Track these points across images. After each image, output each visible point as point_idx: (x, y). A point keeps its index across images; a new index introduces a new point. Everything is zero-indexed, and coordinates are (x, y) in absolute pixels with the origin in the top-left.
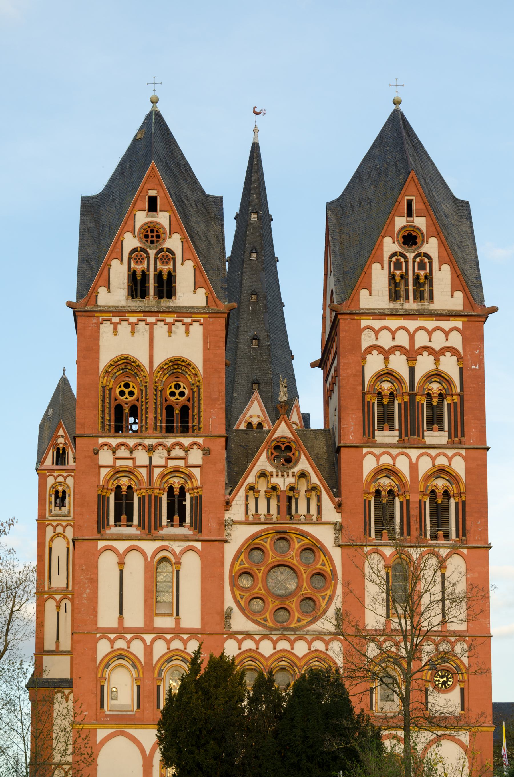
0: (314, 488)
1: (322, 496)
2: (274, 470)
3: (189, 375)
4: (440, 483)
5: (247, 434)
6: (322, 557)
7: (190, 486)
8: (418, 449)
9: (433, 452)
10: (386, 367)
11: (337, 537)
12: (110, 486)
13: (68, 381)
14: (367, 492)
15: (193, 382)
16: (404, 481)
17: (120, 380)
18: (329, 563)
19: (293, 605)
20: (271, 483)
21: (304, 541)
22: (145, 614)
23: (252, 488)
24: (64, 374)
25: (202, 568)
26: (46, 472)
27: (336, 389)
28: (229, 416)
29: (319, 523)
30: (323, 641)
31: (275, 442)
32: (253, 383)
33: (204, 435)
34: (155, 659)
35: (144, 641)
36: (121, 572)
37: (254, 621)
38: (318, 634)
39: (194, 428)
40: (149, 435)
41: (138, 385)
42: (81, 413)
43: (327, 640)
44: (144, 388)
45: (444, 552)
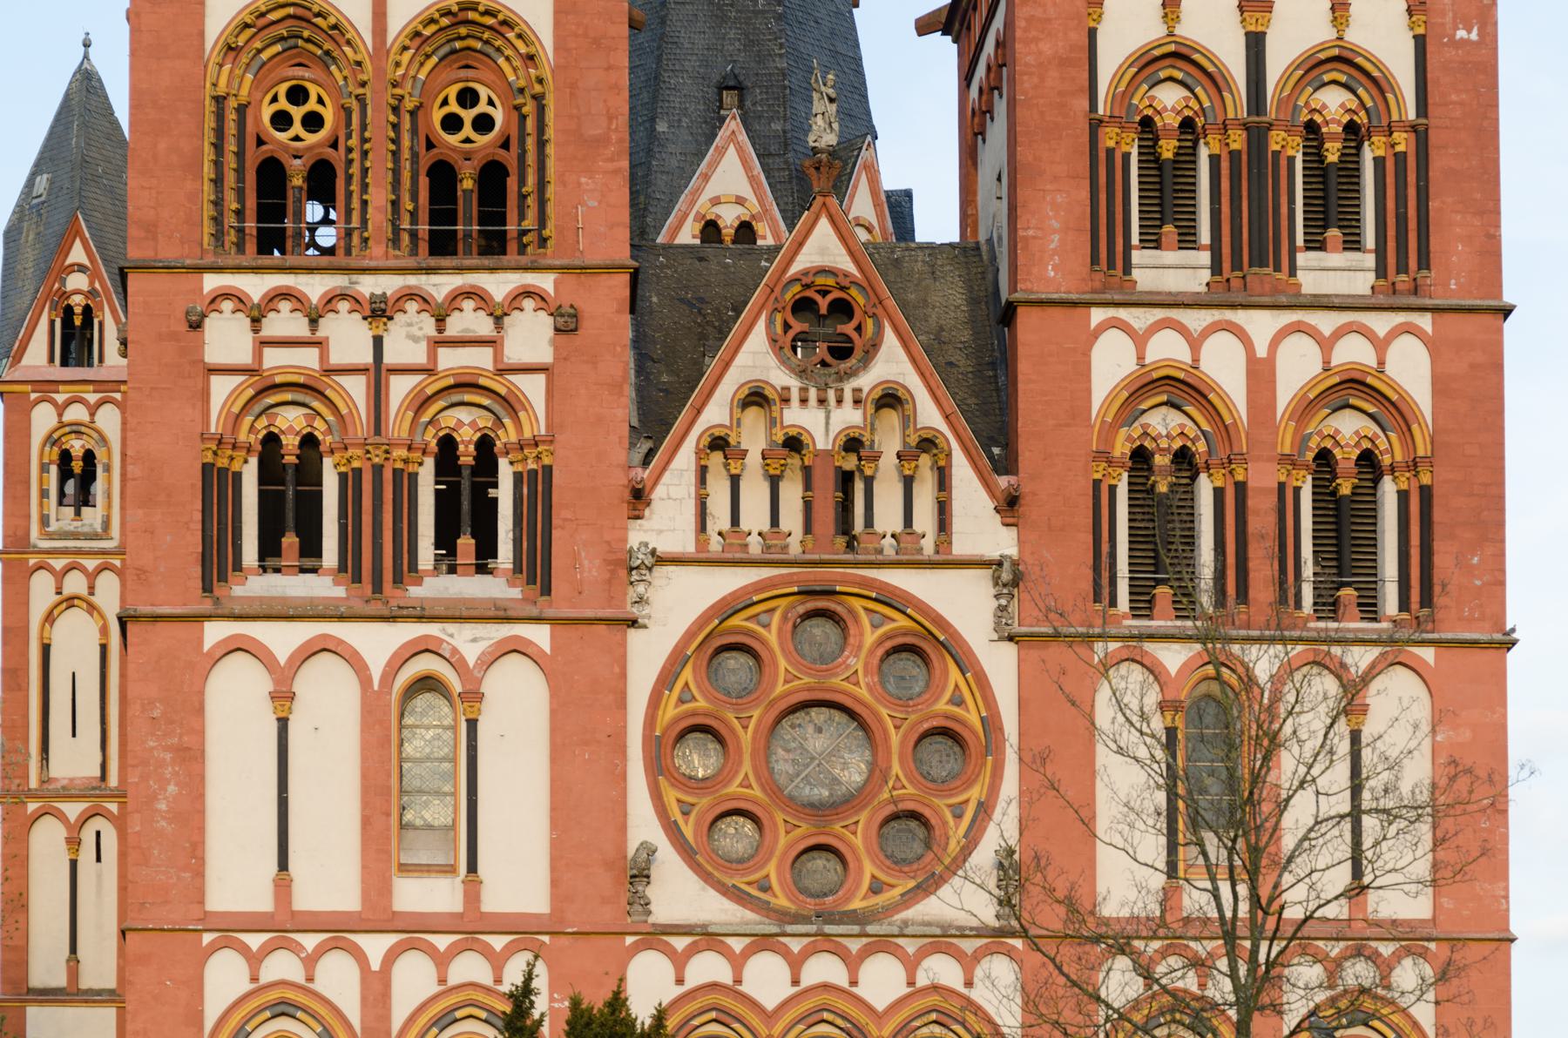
0: (928, 444)
1: (954, 470)
2: (794, 383)
3: (507, 59)
4: (1349, 427)
5: (701, 259)
7: (513, 438)
8: (1275, 312)
9: (1327, 322)
10: (1171, 34)
11: (1002, 609)
12: (243, 436)
13: (99, 80)
14: (1104, 456)
15: (522, 83)
16: (1228, 421)
17: (274, 76)
18: (977, 695)
19: (857, 835)
20: (783, 427)
21: (893, 620)
22: (364, 867)
23: (718, 443)
24: (86, 57)
25: (553, 712)
26: (29, 388)
27: (1001, 107)
28: (642, 198)
29: (945, 562)
30: (958, 955)
31: (797, 288)
32: (722, 87)
33: (557, 262)
34: (398, 1017)
36: (283, 724)
38: (938, 931)
39: (525, 240)
40: (373, 264)
41: (337, 92)
42: (143, 187)
43: (969, 951)
44: (355, 105)
45: (1360, 658)
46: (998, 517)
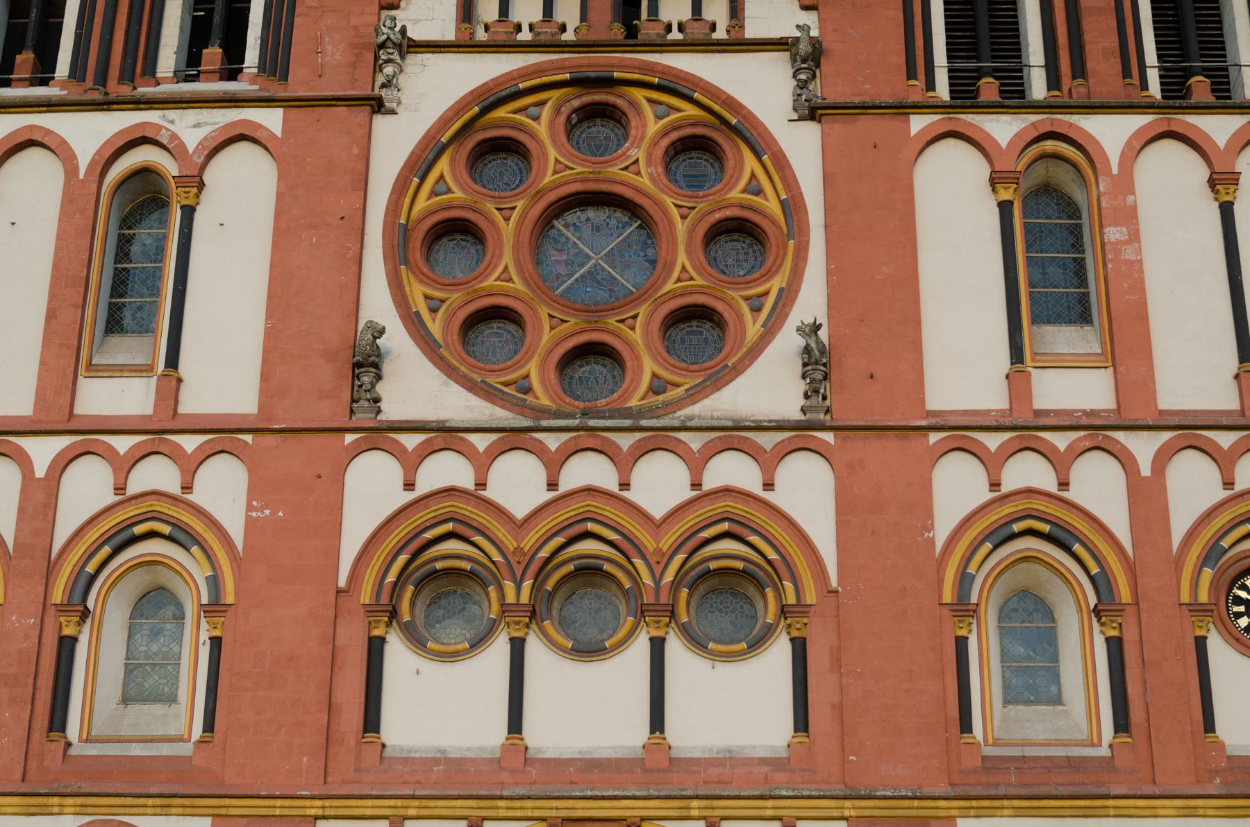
6: (750, 162)
11: (802, 85)
18: (776, 178)
21: (680, 110)
22: (42, 363)
25: (280, 196)
29: (738, 44)
30: (754, 452)
34: (63, 532)
35: (24, 462)
37: (471, 386)
43: (768, 447)
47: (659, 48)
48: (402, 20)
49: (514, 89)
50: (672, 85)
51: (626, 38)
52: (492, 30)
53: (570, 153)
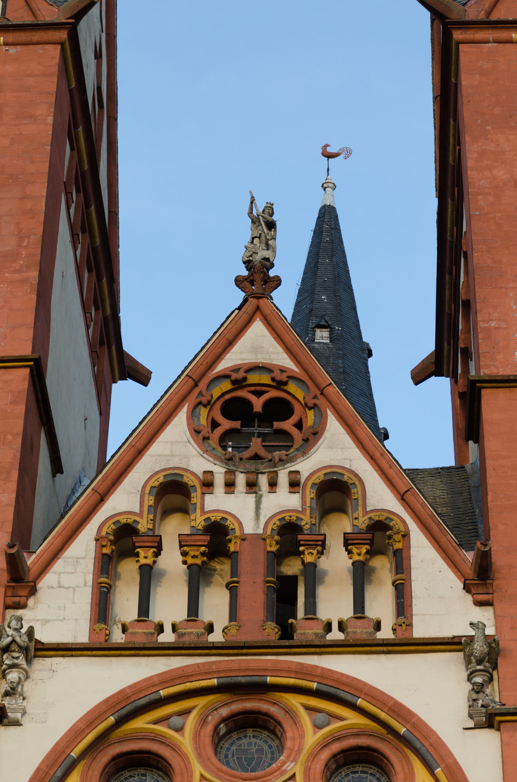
1: (413, 552)
20: (203, 512)
21: (341, 719)
31: (226, 385)
46: (469, 598)
47: (317, 650)
48: (30, 621)
49: (154, 697)
50: (332, 690)
51: (279, 639)
52: (130, 631)
53: (217, 768)
